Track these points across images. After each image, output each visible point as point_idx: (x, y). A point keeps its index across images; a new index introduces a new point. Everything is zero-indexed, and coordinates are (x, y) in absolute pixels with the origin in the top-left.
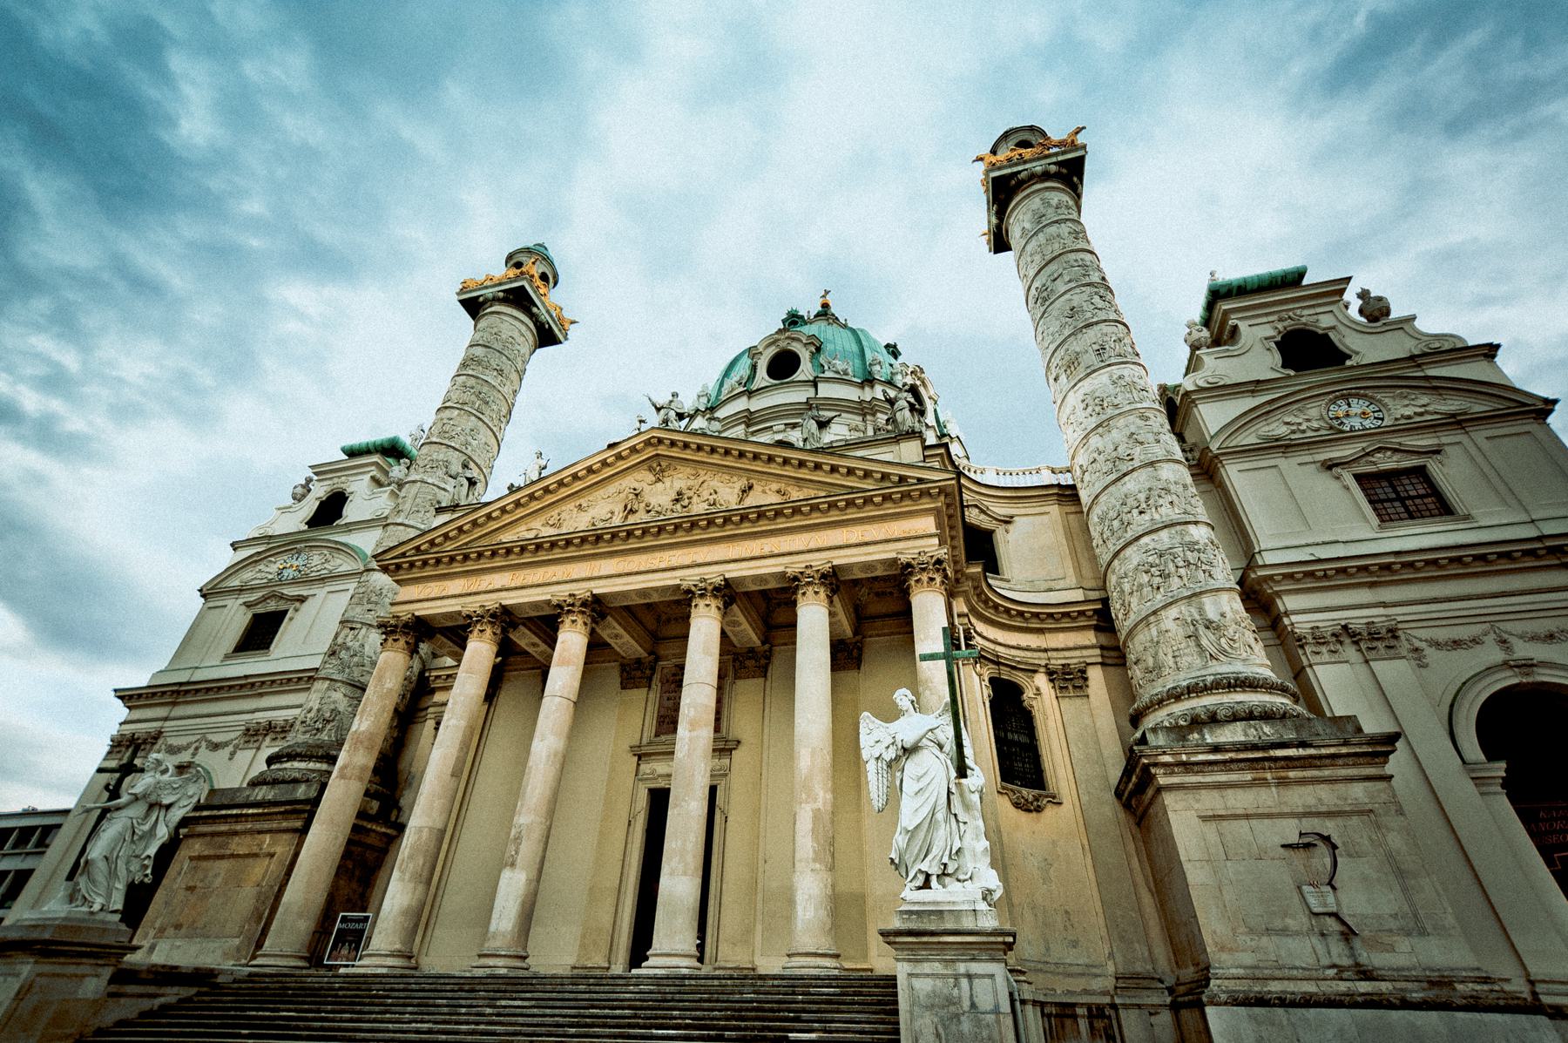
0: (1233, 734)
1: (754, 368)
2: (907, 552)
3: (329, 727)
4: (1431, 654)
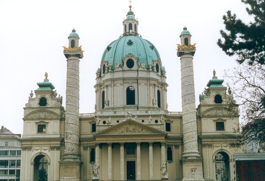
0: (190, 158)
1: (123, 62)
2: (161, 141)
4: (215, 148)
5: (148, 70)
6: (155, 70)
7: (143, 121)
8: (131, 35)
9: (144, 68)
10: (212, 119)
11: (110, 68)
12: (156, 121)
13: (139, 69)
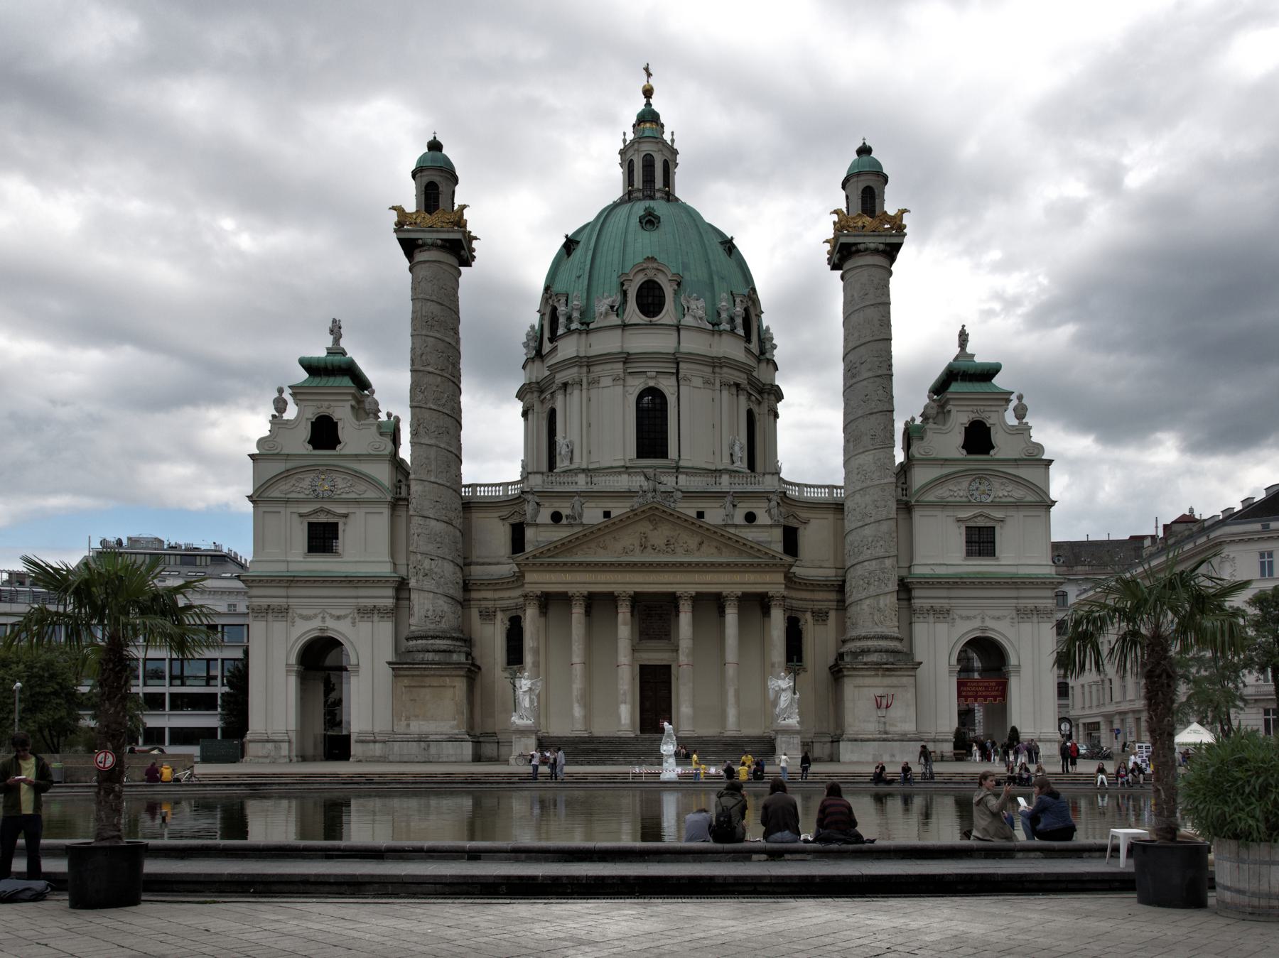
0: (874, 658)
3: (444, 621)
5: (716, 328)
6: (741, 331)
7: (701, 515)
8: (652, 198)
9: (701, 319)
10: (951, 514)
11: (576, 315)
12: (750, 517)
13: (682, 323)
